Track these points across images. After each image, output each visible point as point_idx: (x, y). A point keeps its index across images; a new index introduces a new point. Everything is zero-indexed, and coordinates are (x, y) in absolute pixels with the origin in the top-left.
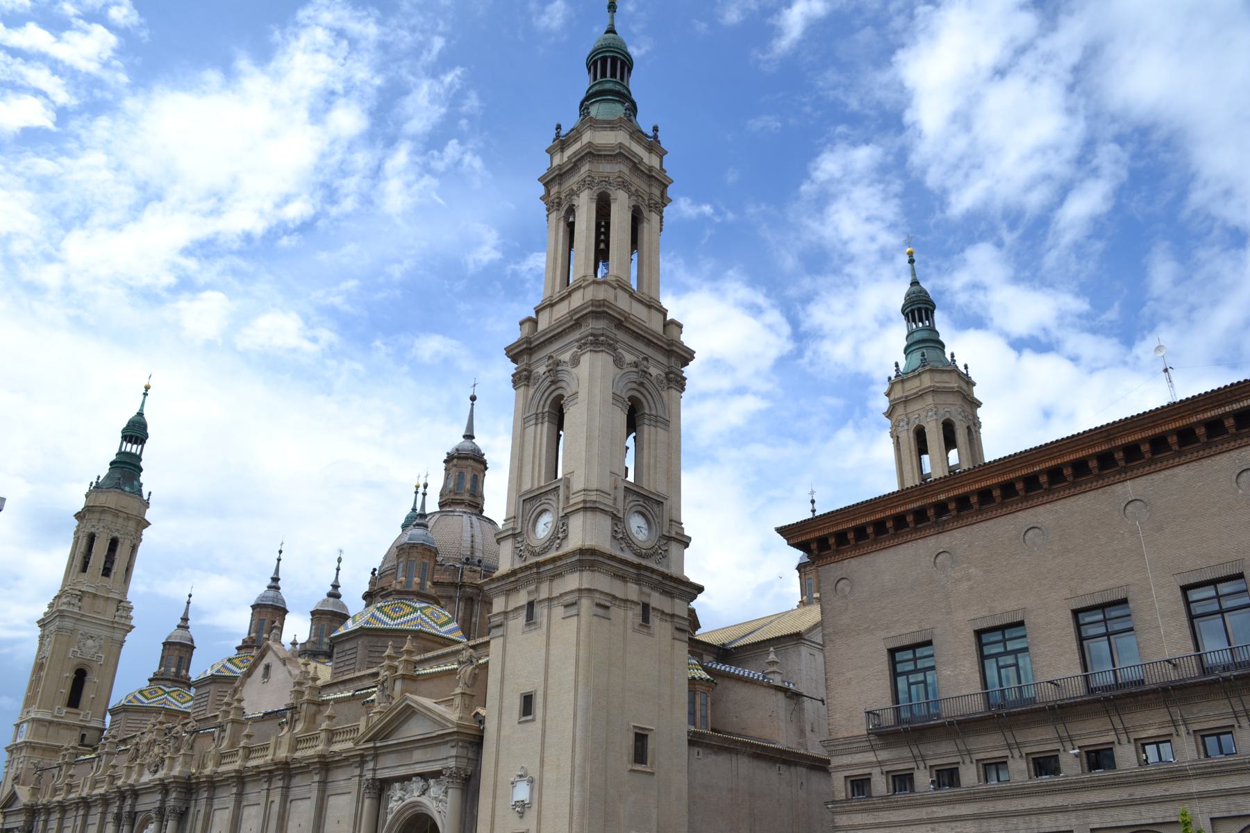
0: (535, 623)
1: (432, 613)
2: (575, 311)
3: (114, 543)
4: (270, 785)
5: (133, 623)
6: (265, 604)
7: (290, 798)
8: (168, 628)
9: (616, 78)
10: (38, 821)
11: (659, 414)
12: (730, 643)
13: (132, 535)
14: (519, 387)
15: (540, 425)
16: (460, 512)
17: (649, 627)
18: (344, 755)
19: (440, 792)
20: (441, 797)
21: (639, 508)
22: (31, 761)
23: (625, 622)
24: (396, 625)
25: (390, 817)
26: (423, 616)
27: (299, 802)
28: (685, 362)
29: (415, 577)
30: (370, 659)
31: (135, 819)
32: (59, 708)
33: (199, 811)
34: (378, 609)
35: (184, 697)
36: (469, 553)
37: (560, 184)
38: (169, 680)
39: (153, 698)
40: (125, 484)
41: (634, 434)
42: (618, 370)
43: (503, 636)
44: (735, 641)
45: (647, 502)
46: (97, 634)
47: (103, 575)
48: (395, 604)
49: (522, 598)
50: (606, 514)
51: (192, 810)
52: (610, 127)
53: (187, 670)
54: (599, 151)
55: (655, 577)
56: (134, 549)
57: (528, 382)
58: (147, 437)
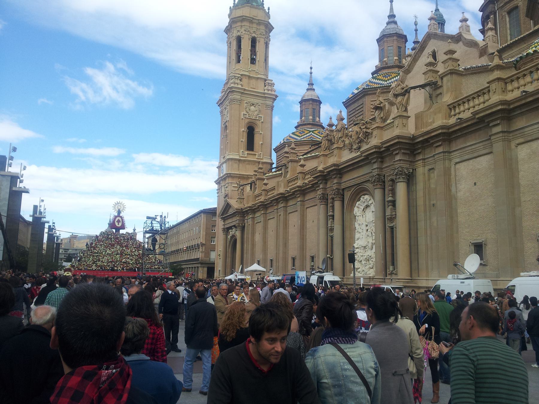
3: (254, 41)
13: (264, 35)
22: (233, 185)
38: (309, 124)
39: (302, 136)
46: (256, 102)
53: (319, 119)
56: (267, 45)
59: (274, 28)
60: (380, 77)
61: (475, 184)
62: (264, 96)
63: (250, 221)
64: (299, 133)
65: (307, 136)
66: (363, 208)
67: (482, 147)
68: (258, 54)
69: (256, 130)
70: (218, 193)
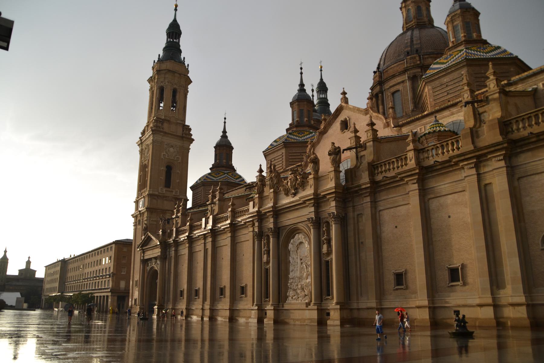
5: (192, 137)
7: (517, 176)
8: (217, 138)
10: (169, 252)
13: (184, 87)
29: (474, 32)
30: (478, 84)
32: (161, 188)
38: (223, 167)
51: (351, 215)
59: (192, 82)
61: (396, 227)
63: (173, 253)
64: (215, 174)
65: (222, 178)
66: (297, 245)
67: (402, 199)
68: (178, 103)
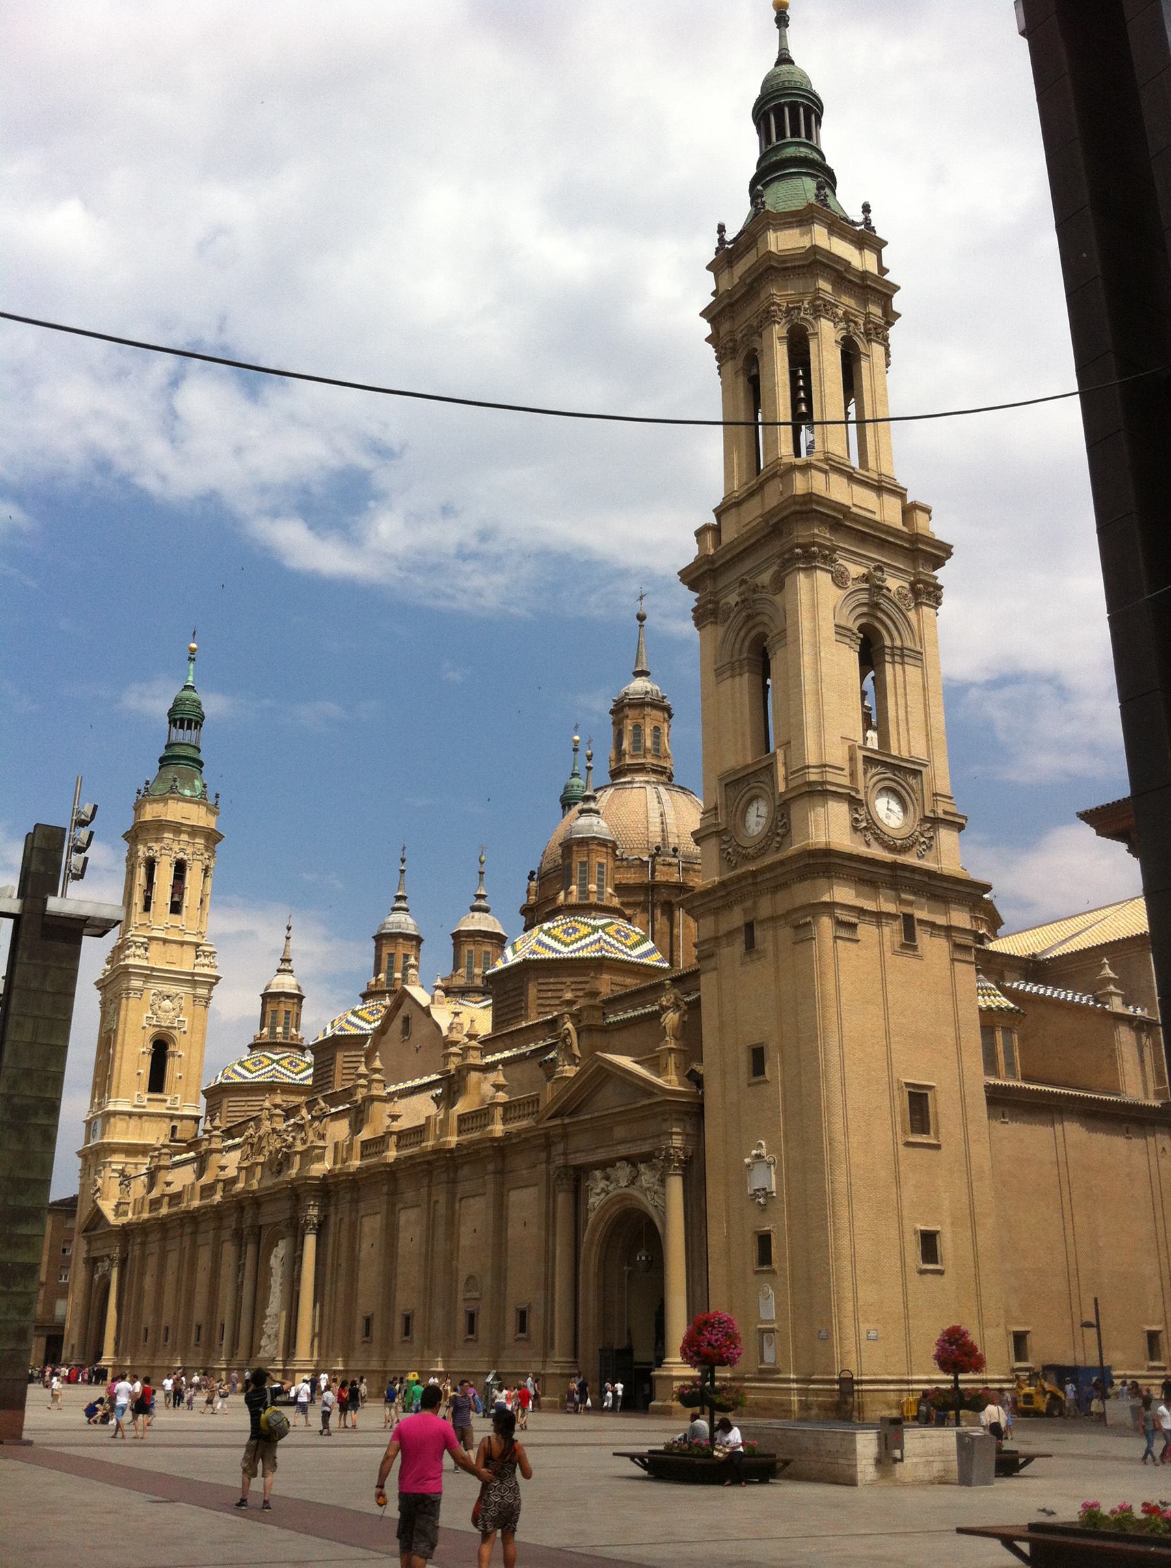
0: (757, 952)
1: (618, 932)
2: (772, 513)
3: (180, 868)
4: (430, 1181)
6: (391, 933)
7: (459, 1196)
9: (799, 136)
11: (906, 645)
12: (1043, 952)
14: (705, 626)
15: (737, 678)
16: (640, 782)
17: (915, 948)
18: (523, 1136)
19: (652, 1180)
20: (656, 1187)
21: (887, 783)
23: (881, 943)
24: (571, 952)
25: (592, 1216)
26: (605, 937)
27: (472, 1201)
28: (938, 563)
30: (540, 1001)
31: (259, 1235)
33: (341, 1219)
34: (547, 933)
35: (298, 1065)
36: (659, 840)
37: (732, 318)
40: (183, 787)
41: (872, 674)
42: (841, 592)
43: (715, 969)
44: (1051, 949)
45: (897, 773)
47: (171, 912)
48: (567, 923)
49: (736, 918)
50: (840, 798)
51: (332, 1219)
52: (796, 221)
54: (784, 262)
55: (917, 877)
57: (716, 618)
58: (203, 718)
60: (363, 1014)
62: (192, 980)
68: (187, 893)
69: (171, 1048)
70: (81, 1177)
